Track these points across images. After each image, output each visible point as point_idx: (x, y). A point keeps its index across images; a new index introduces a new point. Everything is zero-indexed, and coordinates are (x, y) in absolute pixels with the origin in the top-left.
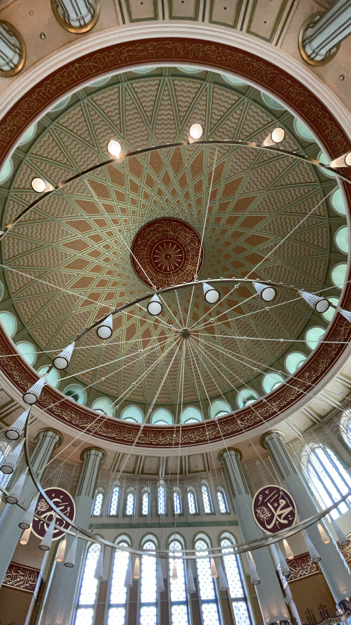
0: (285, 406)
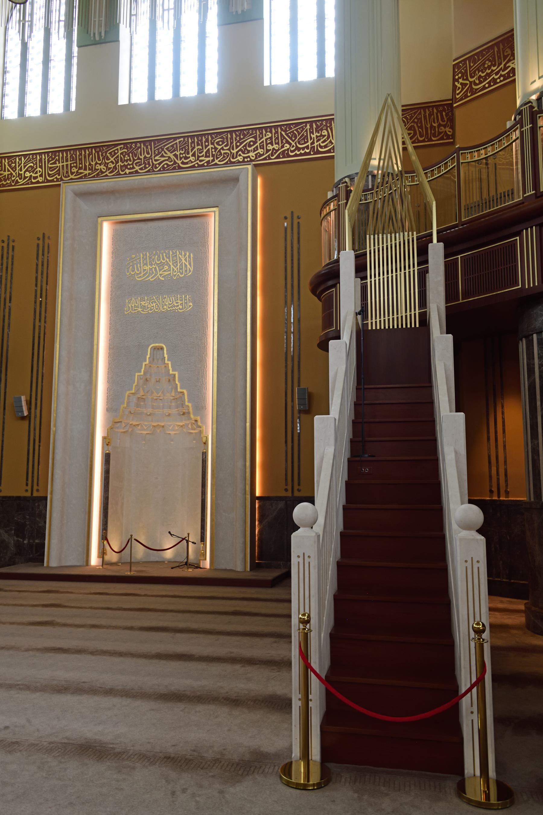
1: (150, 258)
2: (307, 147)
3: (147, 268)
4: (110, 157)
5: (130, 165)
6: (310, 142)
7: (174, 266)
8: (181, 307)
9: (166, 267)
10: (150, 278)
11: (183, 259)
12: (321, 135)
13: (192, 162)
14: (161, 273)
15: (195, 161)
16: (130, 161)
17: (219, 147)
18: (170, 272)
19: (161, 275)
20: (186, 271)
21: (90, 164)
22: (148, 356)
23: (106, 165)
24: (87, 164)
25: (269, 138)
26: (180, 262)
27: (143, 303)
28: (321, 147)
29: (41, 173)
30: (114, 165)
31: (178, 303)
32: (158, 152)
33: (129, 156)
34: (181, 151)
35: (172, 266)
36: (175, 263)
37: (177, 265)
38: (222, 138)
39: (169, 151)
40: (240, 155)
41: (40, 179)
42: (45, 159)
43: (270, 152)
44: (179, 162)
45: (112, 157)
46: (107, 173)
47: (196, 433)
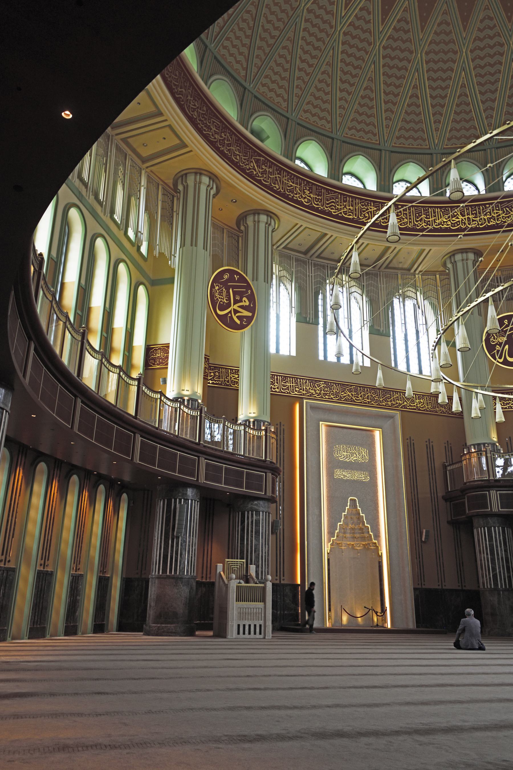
0: (317, 210)
1: (346, 449)
2: (415, 406)
6: (416, 404)
8: (363, 478)
12: (420, 402)
17: (374, 396)
19: (352, 459)
20: (365, 459)
21: (306, 388)
22: (349, 504)
23: (315, 391)
24: (305, 388)
27: (344, 473)
28: (421, 407)
36: (359, 454)
38: (374, 391)
40: (384, 402)
41: (276, 390)
42: (280, 379)
46: (316, 395)
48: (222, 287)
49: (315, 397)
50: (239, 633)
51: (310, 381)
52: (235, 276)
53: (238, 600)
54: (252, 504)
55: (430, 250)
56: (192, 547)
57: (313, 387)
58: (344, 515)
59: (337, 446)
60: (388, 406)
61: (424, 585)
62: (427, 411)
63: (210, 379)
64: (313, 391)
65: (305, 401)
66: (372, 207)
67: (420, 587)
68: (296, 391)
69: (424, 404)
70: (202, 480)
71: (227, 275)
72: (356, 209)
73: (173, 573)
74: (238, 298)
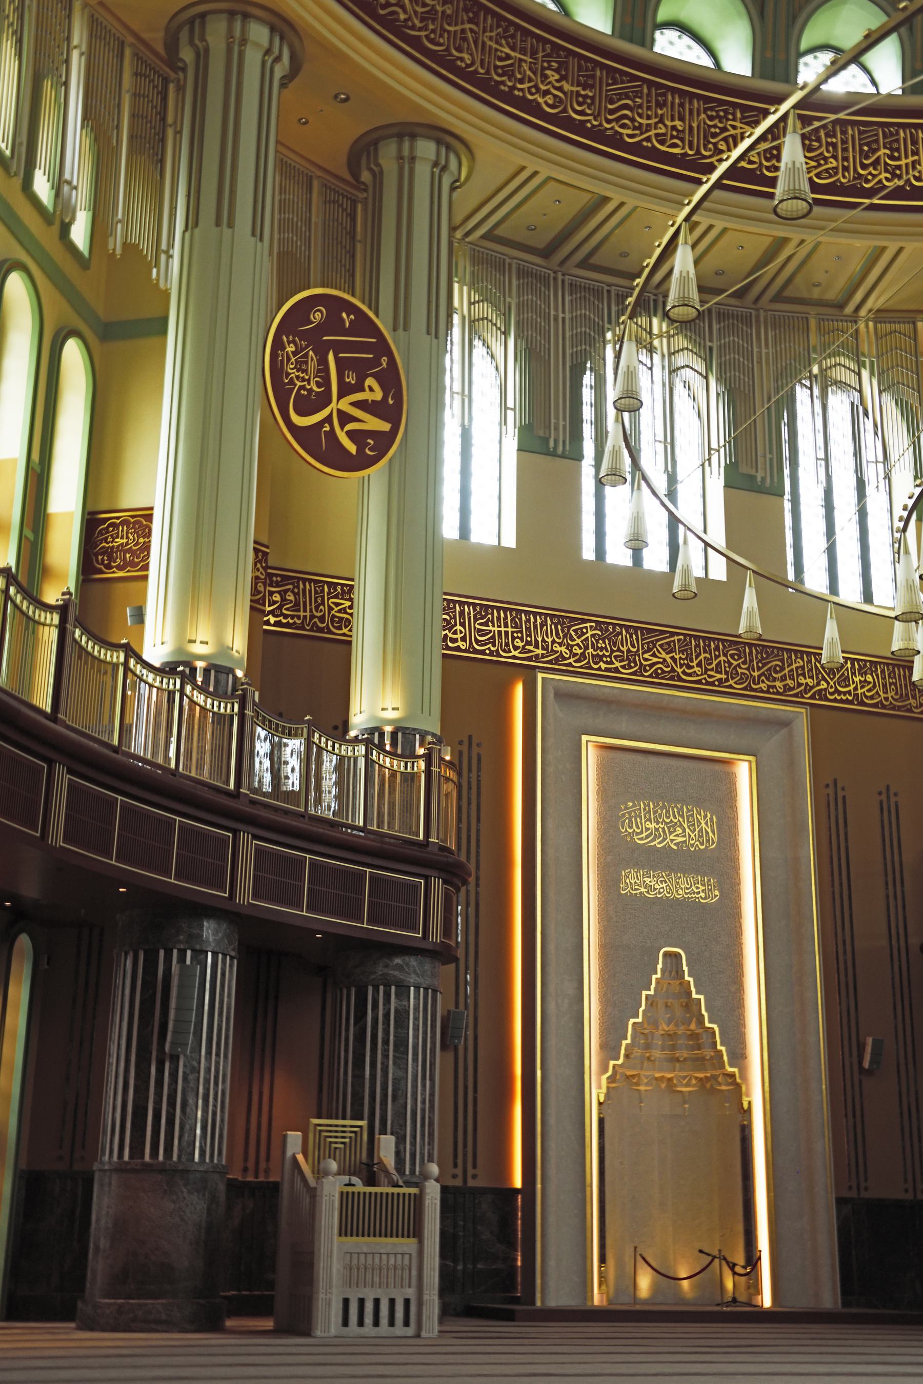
0: (579, 128)
1: (655, 812)
2: (849, 693)
3: (652, 826)
4: (575, 637)
5: (606, 657)
6: (852, 687)
7: (690, 830)
8: (703, 895)
9: (679, 831)
10: (655, 842)
11: (703, 822)
13: (698, 675)
14: (672, 837)
15: (702, 675)
16: (607, 651)
17: (735, 663)
18: (684, 839)
19: (672, 841)
20: (708, 841)
21: (543, 640)
22: (660, 966)
23: (569, 647)
24: (540, 639)
25: (801, 667)
26: (698, 826)
27: (647, 880)
28: (867, 697)
29: (462, 635)
30: (582, 651)
31: (698, 888)
32: (648, 647)
33: (605, 643)
34: (681, 655)
35: (687, 830)
36: (692, 827)
37: (695, 830)
38: (737, 649)
39: (664, 650)
40: (763, 682)
41: (460, 643)
42: (469, 614)
43: (803, 687)
44: (680, 670)
45: (579, 638)
46: (571, 660)
47: (690, 1092)
48: (307, 347)
49: (570, 665)
50: (345, 1323)
51: (556, 620)
52: (344, 315)
53: (345, 1230)
54: (386, 966)
55: (901, 250)
56: (216, 1084)
57: (565, 636)
58: (647, 997)
59: (630, 804)
60: (773, 693)
61: (866, 1189)
62: (884, 707)
63: (272, 612)
64: (563, 649)
65: (540, 676)
66: (738, 124)
67: (853, 1194)
68: (516, 648)
69: (874, 686)
70: (245, 896)
71: (319, 311)
72: (691, 128)
73: (161, 1158)
74: (351, 379)
